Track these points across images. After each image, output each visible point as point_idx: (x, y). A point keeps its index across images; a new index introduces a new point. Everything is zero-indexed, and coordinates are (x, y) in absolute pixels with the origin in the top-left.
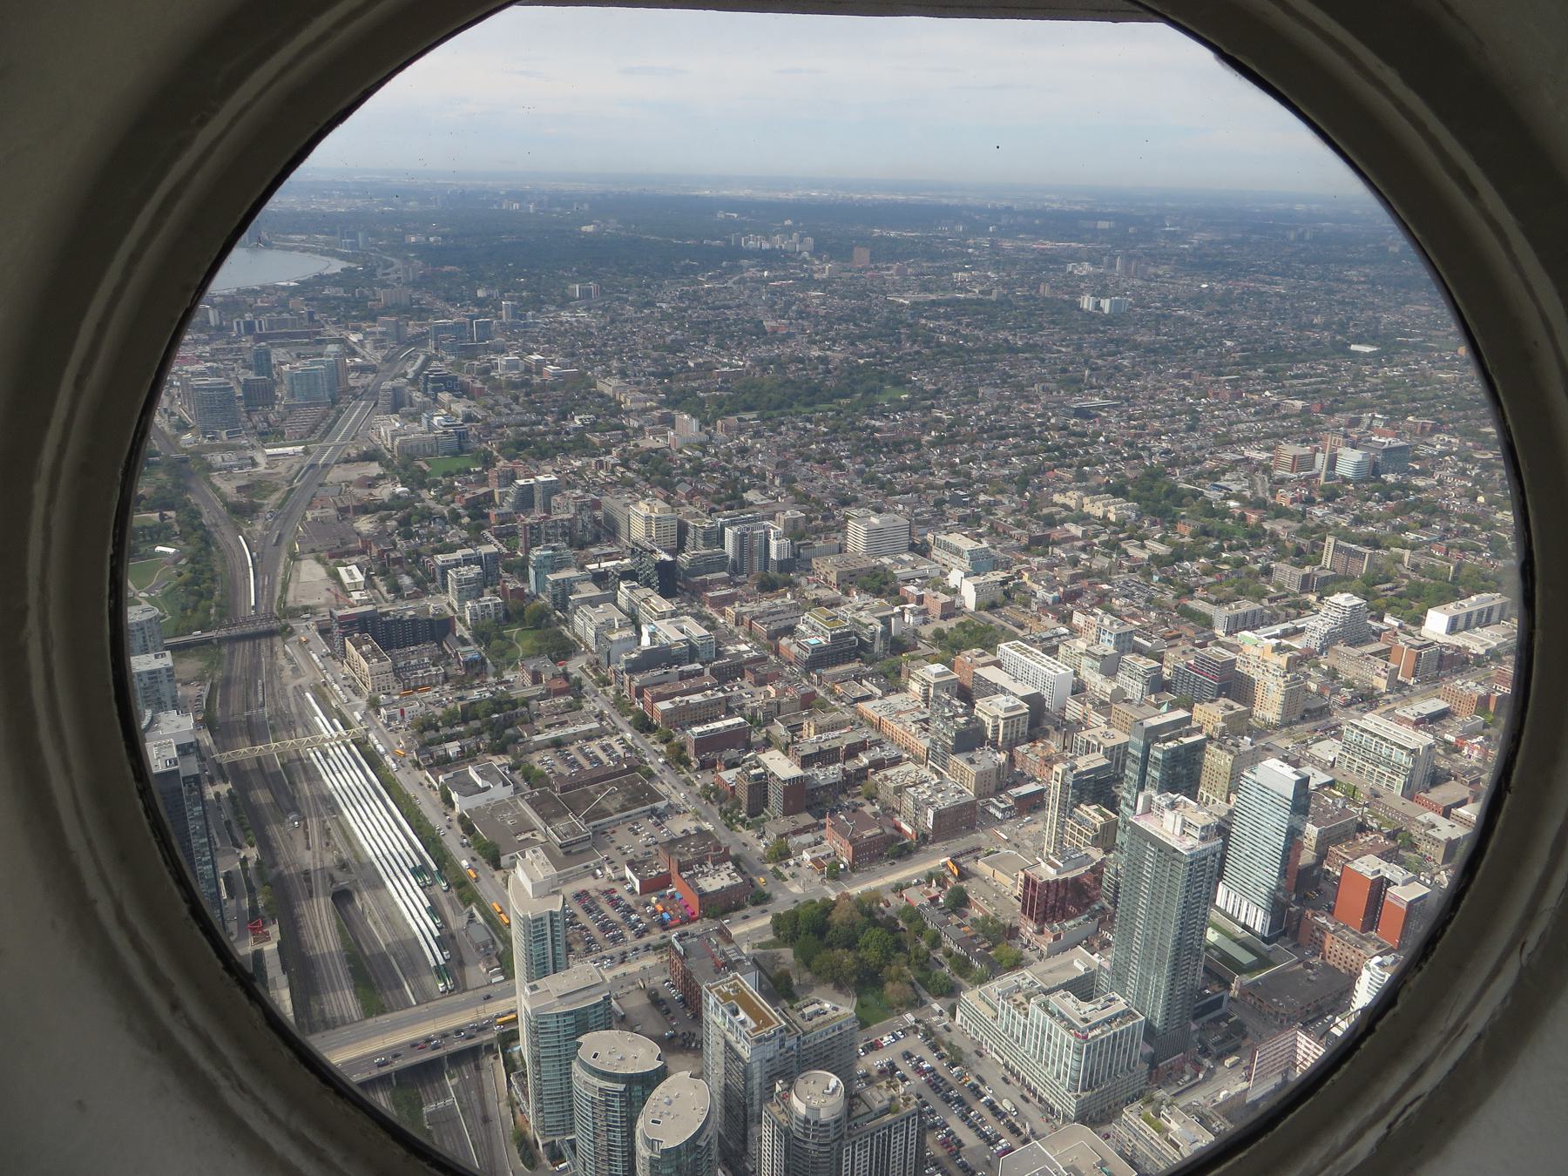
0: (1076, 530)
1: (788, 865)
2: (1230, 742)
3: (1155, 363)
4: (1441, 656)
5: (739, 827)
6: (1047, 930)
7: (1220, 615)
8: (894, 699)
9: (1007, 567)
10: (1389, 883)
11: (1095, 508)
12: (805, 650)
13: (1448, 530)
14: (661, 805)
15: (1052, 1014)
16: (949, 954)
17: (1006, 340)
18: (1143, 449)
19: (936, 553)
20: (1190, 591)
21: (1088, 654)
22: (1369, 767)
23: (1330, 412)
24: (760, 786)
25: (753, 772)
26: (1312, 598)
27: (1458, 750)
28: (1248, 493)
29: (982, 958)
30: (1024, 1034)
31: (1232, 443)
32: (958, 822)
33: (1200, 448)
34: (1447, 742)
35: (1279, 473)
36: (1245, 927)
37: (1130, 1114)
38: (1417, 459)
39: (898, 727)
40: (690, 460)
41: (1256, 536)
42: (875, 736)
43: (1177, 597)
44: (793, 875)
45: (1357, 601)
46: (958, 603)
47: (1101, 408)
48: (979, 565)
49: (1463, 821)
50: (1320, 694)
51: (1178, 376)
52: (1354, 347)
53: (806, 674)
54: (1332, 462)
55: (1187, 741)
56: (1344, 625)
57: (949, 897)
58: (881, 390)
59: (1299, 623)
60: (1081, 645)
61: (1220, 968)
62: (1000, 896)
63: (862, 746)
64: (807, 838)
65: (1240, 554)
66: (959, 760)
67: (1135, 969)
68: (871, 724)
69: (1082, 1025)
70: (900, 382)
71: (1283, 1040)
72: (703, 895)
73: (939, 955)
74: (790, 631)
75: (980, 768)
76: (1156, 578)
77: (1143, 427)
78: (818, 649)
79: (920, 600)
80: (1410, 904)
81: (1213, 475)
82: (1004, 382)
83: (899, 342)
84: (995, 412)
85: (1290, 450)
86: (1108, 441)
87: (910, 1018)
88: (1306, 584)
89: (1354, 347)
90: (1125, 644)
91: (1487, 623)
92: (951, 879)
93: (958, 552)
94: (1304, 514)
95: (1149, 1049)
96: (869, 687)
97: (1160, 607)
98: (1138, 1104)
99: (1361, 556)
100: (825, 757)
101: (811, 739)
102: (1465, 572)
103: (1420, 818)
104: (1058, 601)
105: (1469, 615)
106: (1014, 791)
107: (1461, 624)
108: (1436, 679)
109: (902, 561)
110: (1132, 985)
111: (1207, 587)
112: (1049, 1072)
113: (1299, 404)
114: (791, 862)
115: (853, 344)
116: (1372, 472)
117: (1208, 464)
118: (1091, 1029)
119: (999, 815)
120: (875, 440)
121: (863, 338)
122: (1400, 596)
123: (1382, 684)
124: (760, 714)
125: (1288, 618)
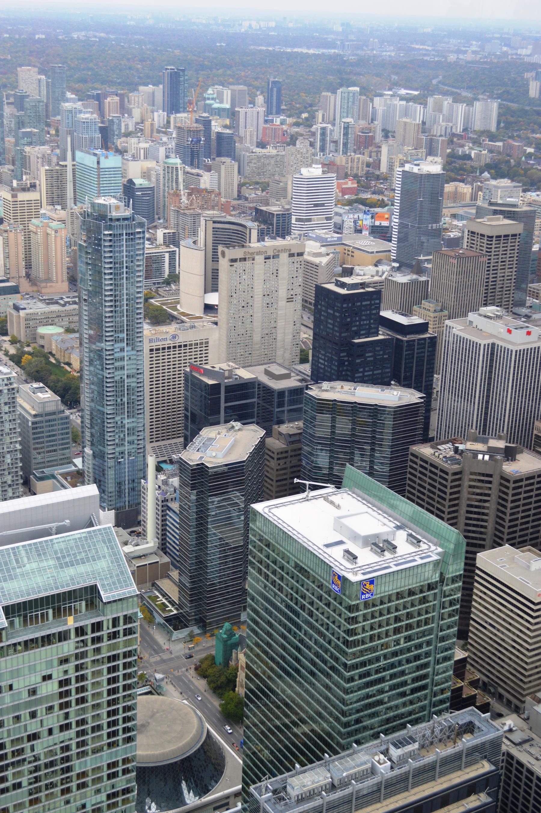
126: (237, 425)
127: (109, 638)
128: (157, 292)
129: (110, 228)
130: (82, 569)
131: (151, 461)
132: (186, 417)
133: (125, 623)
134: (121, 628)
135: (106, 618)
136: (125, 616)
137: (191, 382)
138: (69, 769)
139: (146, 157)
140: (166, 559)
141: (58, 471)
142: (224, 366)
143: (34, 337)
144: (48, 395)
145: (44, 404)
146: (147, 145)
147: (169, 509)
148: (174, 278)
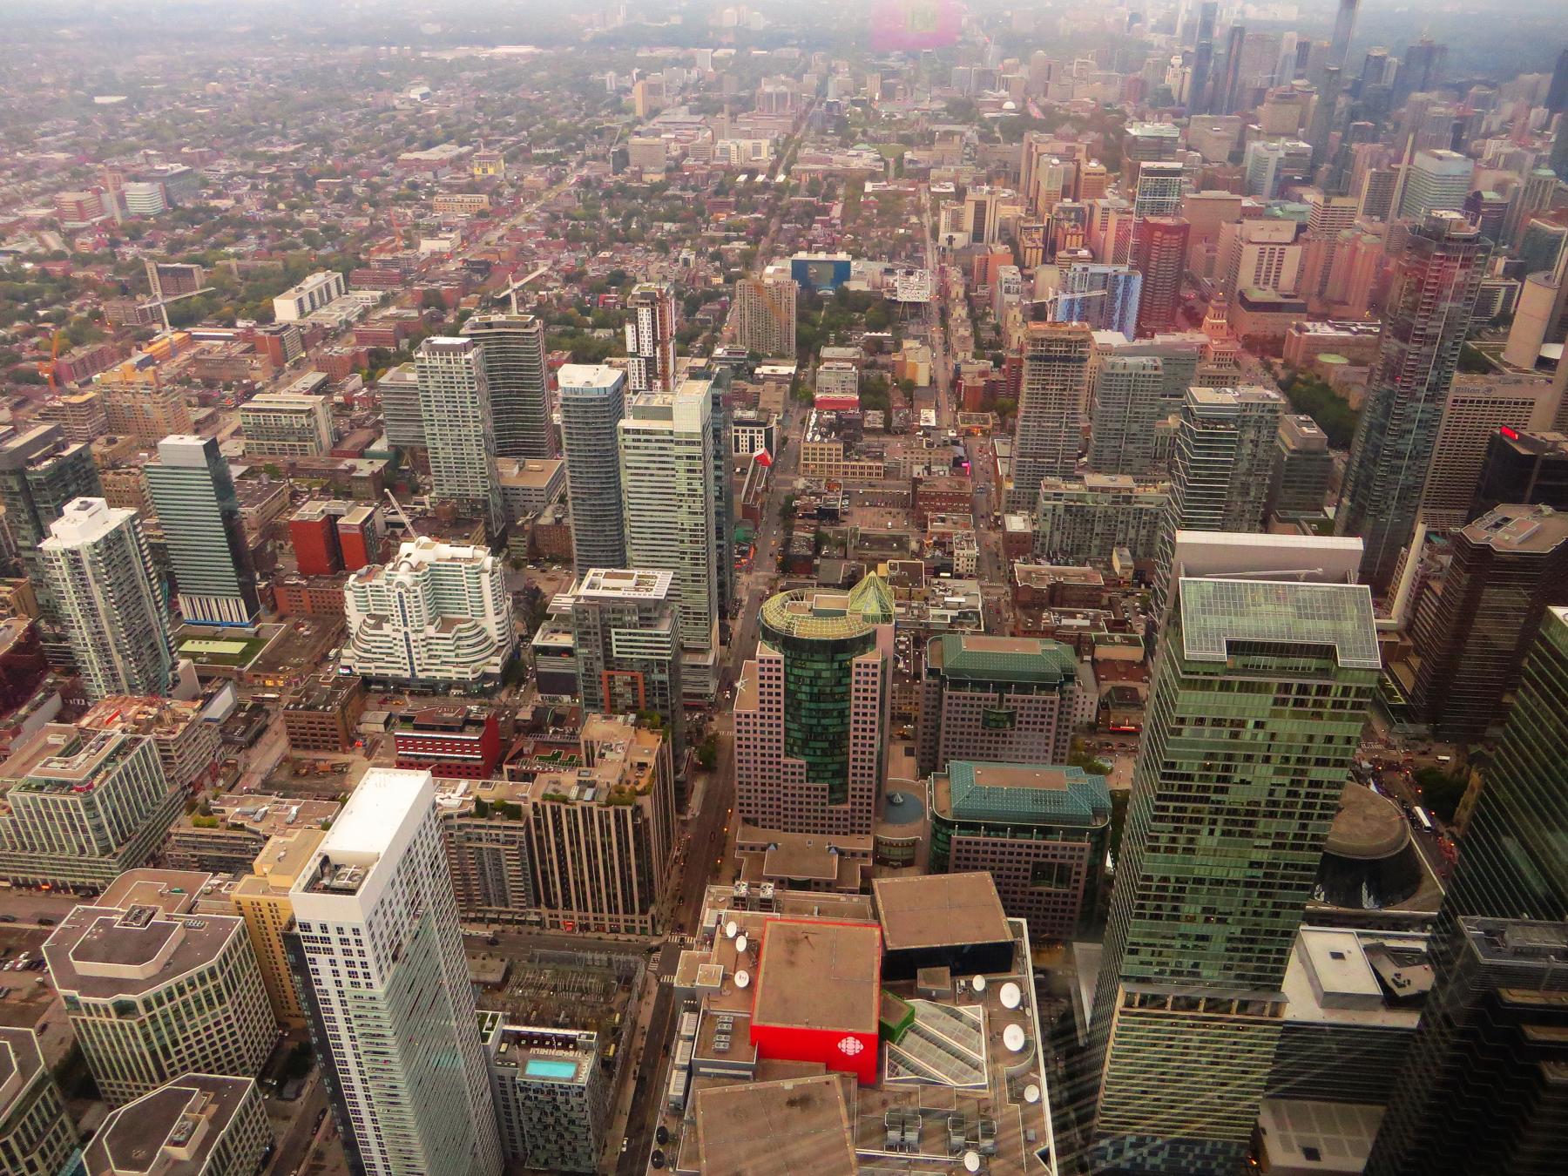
10: (336, 517)
13: (262, 237)
15: (40, 788)
20: (19, 359)
28: (41, 250)
35: (69, 225)
41: (68, 289)
49: (379, 456)
52: (98, 100)
54: (122, 200)
55: (66, 453)
65: (57, 307)
85: (69, 197)
89: (98, 100)
94: (113, 255)
103: (342, 467)
107: (308, 307)
126: (1547, 510)
127: (1333, 707)
128: (1478, 333)
129: (1443, 248)
130: (1325, 625)
131: (1420, 530)
132: (1478, 488)
133: (1356, 696)
134: (1351, 699)
135: (1336, 686)
136: (1358, 689)
137: (1498, 447)
138: (1251, 824)
139: (1506, 167)
140: (1409, 643)
141: (1303, 516)
142: (1552, 436)
143: (1311, 362)
144: (1312, 431)
145: (1308, 439)
146: (1510, 150)
147: (1429, 588)
148: (1506, 319)
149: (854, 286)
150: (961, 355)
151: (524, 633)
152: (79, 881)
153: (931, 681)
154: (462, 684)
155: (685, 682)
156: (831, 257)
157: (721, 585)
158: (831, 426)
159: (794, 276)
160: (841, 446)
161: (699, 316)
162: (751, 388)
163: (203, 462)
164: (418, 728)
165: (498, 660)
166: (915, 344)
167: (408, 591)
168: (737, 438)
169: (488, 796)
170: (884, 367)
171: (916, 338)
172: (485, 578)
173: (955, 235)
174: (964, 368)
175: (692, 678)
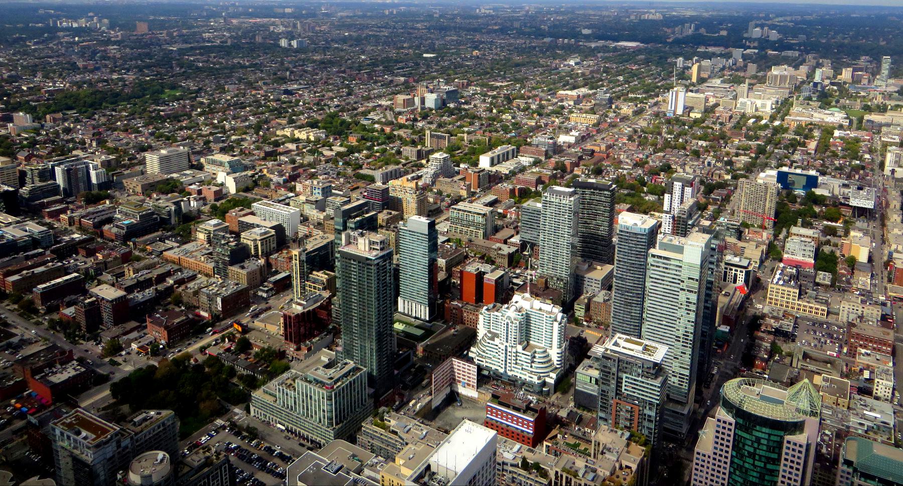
0: (291, 146)
1: (121, 355)
2: (392, 226)
3: (326, 68)
4: (490, 176)
5: (81, 342)
6: (303, 346)
7: (378, 174)
8: (187, 247)
9: (253, 168)
10: (484, 273)
11: (302, 135)
12: (122, 228)
13: (482, 125)
14: (15, 340)
15: (310, 382)
16: (241, 377)
17: (239, 63)
18: (325, 105)
19: (208, 168)
20: (361, 167)
21: (308, 201)
22: (465, 229)
23: (417, 81)
24: (94, 311)
25: (87, 301)
26: (424, 162)
27: (505, 216)
28: (383, 120)
29: (261, 373)
30: (295, 403)
31: (371, 98)
32: (237, 303)
33: (356, 103)
34: (500, 214)
35: (397, 110)
36: (416, 318)
37: (368, 426)
38: (462, 97)
39: (192, 260)
40: (26, 139)
41: (390, 138)
42: (176, 267)
43: (354, 170)
44: (125, 361)
45: (445, 155)
46: (224, 191)
47: (299, 89)
48: (234, 168)
49: (514, 244)
50: (435, 203)
51: (338, 72)
52: (425, 55)
53: (124, 243)
54: (423, 101)
56: (441, 168)
57: (237, 345)
58: (162, 92)
59: (419, 173)
60: (302, 198)
61: (408, 340)
62: (270, 336)
63: (169, 274)
64: (135, 334)
65: (384, 146)
66: (235, 269)
67: (357, 343)
68: (174, 263)
69: (329, 382)
70: (174, 87)
71: (445, 366)
72: (54, 387)
73: (235, 380)
74: (110, 220)
75: (249, 270)
76: (341, 163)
77: (323, 96)
78: (130, 227)
79: (199, 192)
80: (496, 281)
81: (365, 114)
82: (240, 82)
83: (172, 68)
84: (237, 96)
85: (401, 98)
86: (304, 104)
87: (219, 422)
88: (420, 155)
89: (425, 55)
90: (327, 192)
91: (508, 159)
92: (238, 335)
93: (221, 164)
95: (372, 390)
96: (169, 243)
97: (345, 176)
98: (370, 418)
99: (444, 138)
100: (142, 285)
101: (130, 276)
102: (493, 140)
104: (285, 182)
105: (499, 156)
106: (272, 279)
107: (496, 161)
108: (489, 188)
109: (185, 175)
110: (357, 353)
111: (368, 163)
112: (314, 421)
113: (402, 79)
114: (124, 353)
115: (141, 70)
116: (442, 105)
117: (360, 110)
118: (336, 382)
119: (265, 295)
120: (163, 117)
121: (148, 67)
122: (466, 154)
123: (464, 193)
124: (92, 271)
125: (413, 171)
149: (818, 192)
150: (894, 247)
151: (573, 363)
152: (314, 437)
153: (845, 468)
154: (531, 385)
155: (667, 421)
156: (805, 172)
157: (701, 364)
158: (791, 277)
159: (778, 182)
160: (797, 291)
161: (713, 196)
162: (741, 244)
163: (426, 231)
164: (500, 404)
165: (554, 375)
166: (860, 234)
167: (512, 322)
168: (725, 273)
169: (531, 458)
170: (836, 245)
171: (860, 230)
172: (556, 325)
173: (896, 169)
174: (895, 255)
175: (671, 419)
